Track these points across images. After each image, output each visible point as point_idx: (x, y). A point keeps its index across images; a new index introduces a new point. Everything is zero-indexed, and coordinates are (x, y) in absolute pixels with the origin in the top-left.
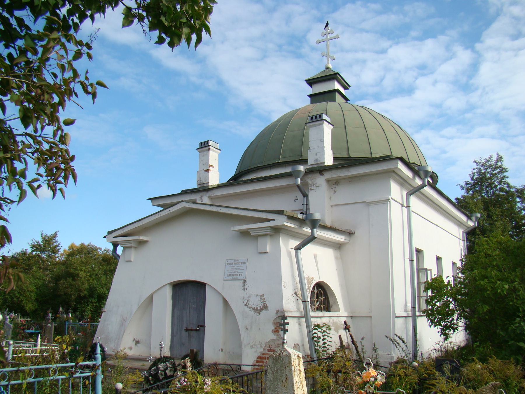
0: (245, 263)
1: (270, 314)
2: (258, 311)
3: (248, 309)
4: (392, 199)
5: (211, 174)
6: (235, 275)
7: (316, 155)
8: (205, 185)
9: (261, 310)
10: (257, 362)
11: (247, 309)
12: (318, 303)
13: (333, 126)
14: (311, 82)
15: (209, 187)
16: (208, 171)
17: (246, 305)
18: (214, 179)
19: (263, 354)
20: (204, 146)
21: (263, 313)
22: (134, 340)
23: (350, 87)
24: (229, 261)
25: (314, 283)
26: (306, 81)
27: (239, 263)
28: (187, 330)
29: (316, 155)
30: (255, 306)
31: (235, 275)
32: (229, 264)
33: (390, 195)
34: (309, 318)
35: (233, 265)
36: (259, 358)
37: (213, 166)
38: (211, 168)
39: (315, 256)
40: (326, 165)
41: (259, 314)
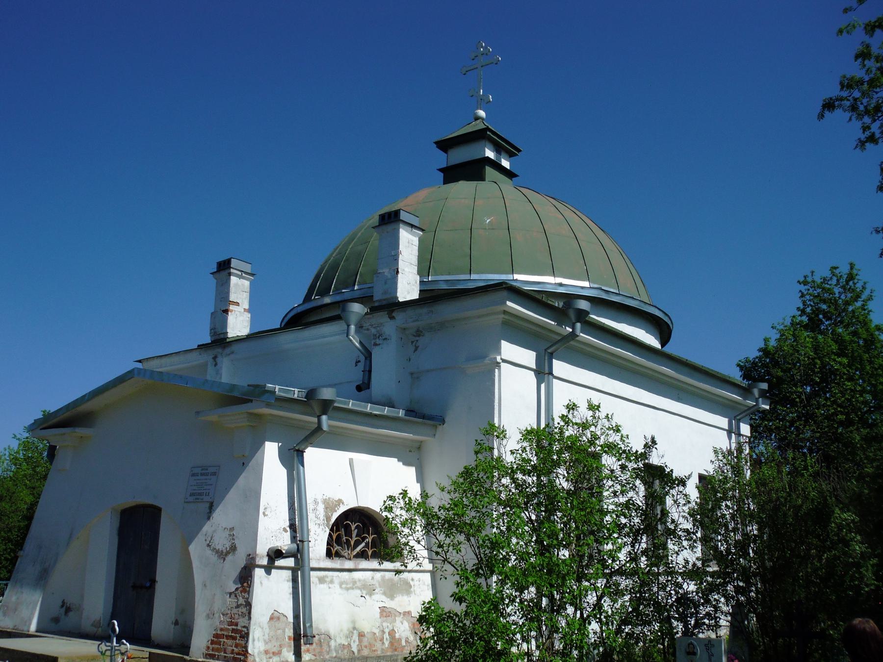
0: (214, 474)
1: (238, 561)
2: (222, 555)
3: (210, 552)
4: (504, 361)
5: (231, 318)
6: (200, 494)
7: (386, 283)
8: (222, 336)
9: (228, 553)
10: (213, 642)
11: (209, 552)
12: (363, 544)
13: (422, 230)
14: (445, 145)
15: (228, 340)
16: (226, 311)
17: (208, 545)
18: (238, 325)
19: (221, 630)
20: (224, 267)
21: (230, 558)
22: (62, 606)
23: (519, 151)
24: (196, 471)
25: (342, 509)
26: (436, 143)
27: (207, 474)
28: (134, 587)
29: (386, 283)
30: (220, 547)
31: (200, 494)
32: (193, 475)
33: (500, 354)
34: (307, 569)
35: (200, 477)
36: (216, 636)
37: (237, 304)
38: (231, 307)
39: (351, 462)
40: (401, 300)
41: (224, 559)
